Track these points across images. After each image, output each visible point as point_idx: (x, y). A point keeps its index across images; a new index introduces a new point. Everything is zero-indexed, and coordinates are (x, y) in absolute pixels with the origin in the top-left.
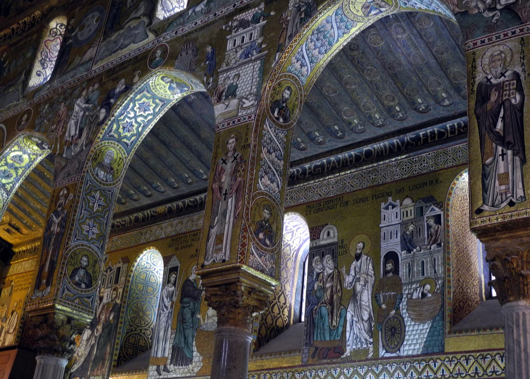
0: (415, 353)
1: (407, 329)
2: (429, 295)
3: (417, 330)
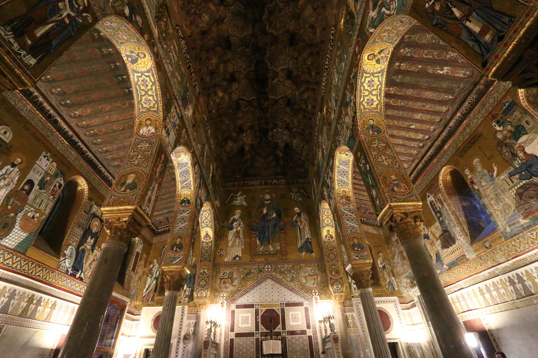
0: (10, 246)
1: (14, 230)
2: (36, 219)
3: (19, 234)
